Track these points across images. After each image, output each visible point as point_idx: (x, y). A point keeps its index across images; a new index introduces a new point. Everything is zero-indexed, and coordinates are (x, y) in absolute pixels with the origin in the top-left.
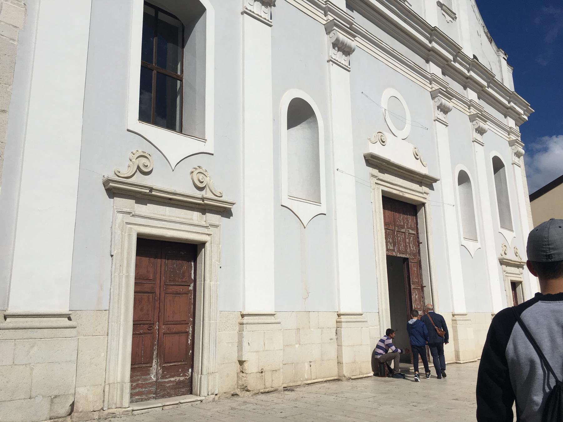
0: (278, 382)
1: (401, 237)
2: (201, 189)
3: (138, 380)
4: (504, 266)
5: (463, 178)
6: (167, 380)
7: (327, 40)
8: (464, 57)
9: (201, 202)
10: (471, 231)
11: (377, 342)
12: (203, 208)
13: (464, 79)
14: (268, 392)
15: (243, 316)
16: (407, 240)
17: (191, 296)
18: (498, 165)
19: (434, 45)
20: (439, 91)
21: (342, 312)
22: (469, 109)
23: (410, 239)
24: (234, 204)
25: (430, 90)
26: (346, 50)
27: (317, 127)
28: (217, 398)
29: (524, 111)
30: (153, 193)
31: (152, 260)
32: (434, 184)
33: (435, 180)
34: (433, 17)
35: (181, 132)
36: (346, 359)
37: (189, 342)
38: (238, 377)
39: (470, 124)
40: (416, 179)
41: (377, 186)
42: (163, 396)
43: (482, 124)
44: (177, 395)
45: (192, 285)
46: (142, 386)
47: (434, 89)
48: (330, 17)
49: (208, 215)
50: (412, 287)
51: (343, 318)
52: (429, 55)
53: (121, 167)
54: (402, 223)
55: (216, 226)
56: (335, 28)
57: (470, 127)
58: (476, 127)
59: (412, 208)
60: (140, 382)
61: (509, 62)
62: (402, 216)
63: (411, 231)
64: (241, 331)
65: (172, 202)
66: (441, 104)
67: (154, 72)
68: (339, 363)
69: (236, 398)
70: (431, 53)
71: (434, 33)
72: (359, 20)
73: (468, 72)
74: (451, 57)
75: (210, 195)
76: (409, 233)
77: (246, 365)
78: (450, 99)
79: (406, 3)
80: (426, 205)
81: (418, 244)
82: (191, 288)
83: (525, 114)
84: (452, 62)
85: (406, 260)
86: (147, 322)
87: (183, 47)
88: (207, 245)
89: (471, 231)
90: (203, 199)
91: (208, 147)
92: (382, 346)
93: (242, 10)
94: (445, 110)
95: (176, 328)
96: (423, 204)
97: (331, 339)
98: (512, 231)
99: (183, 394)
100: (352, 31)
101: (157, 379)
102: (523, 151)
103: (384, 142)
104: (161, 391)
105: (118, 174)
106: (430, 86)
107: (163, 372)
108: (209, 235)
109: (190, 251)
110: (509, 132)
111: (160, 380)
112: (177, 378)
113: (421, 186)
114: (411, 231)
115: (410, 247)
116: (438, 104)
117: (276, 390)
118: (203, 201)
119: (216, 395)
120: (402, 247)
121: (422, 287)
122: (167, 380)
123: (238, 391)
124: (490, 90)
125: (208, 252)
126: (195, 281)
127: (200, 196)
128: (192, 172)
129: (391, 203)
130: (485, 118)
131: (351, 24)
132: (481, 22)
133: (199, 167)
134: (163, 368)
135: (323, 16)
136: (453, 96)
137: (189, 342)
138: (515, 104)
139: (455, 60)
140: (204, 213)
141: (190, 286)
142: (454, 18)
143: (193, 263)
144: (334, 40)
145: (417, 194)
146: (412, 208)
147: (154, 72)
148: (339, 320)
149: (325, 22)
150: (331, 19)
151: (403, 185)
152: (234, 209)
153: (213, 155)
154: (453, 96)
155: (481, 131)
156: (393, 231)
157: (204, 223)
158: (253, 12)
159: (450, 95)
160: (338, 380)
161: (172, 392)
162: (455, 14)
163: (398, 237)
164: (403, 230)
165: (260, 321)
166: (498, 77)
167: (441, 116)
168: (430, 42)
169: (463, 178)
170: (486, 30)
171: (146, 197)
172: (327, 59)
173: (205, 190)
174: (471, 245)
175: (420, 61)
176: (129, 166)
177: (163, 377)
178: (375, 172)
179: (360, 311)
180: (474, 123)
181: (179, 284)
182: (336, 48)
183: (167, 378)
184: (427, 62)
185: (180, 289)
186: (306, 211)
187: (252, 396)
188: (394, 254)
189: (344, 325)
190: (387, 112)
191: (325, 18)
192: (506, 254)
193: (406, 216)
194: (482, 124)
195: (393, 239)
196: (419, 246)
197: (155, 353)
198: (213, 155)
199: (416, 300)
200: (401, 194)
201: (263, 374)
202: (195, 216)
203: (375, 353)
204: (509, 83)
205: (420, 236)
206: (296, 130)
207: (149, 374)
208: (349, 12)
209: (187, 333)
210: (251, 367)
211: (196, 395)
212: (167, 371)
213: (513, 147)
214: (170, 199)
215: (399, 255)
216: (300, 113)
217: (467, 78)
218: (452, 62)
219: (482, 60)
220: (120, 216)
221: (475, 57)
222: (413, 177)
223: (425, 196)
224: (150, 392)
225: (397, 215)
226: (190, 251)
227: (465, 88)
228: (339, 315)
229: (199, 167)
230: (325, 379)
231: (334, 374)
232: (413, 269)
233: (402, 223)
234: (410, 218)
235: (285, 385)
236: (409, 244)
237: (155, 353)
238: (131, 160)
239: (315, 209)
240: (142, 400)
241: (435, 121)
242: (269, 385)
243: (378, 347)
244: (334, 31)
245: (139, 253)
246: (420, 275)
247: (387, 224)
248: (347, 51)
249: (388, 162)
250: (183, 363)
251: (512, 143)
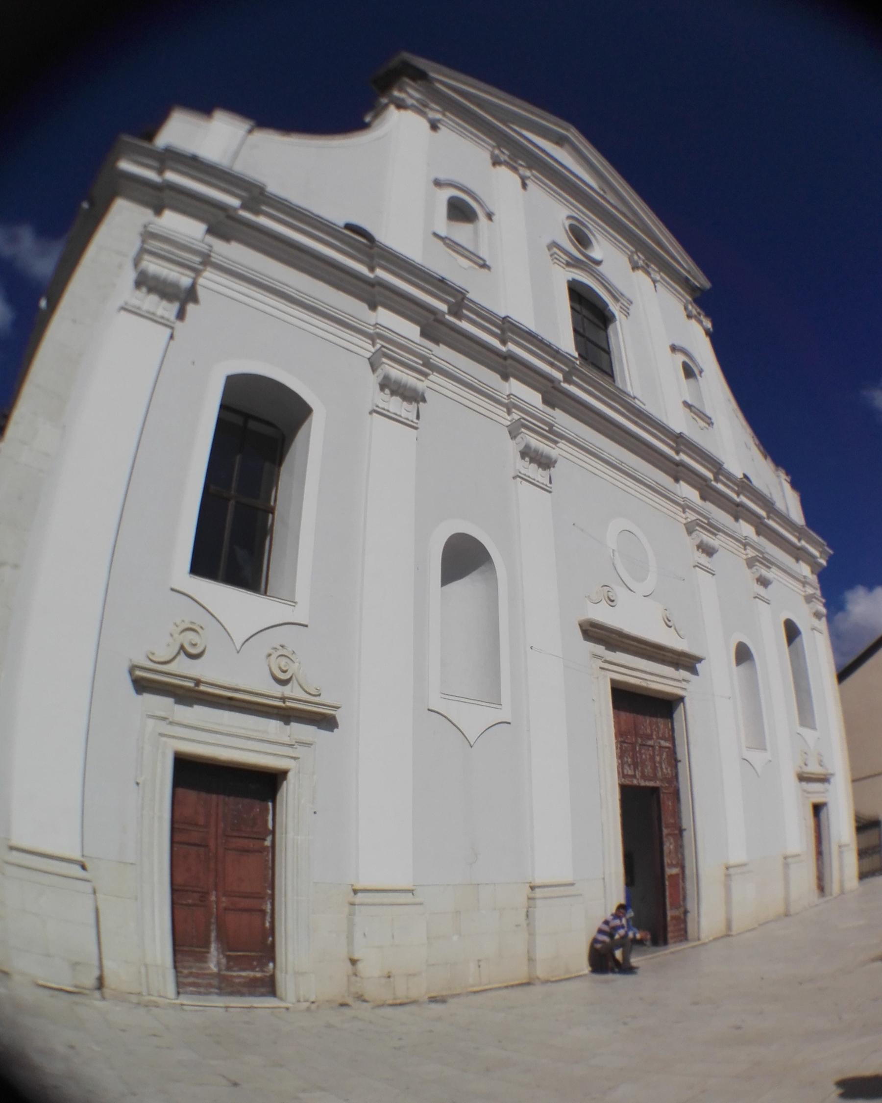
0: (419, 989)
1: (646, 754)
2: (284, 683)
3: (191, 967)
4: (804, 784)
5: (743, 654)
6: (235, 974)
7: (512, 448)
8: (729, 476)
9: (280, 704)
10: (758, 738)
11: (599, 924)
12: (286, 715)
13: (734, 506)
14: (401, 1004)
15: (355, 892)
16: (658, 758)
17: (267, 855)
18: (792, 632)
19: (683, 457)
20: (697, 523)
21: (538, 881)
22: (745, 549)
23: (661, 756)
24: (338, 708)
25: (684, 521)
26: (543, 460)
27: (496, 579)
28: (313, 1006)
29: (821, 553)
30: (202, 688)
31: (204, 795)
32: (698, 666)
33: (699, 660)
34: (679, 421)
35: (265, 593)
36: (542, 953)
37: (267, 925)
38: (349, 981)
39: (748, 572)
41: (603, 672)
42: (232, 994)
43: (764, 572)
44: (252, 994)
45: (269, 838)
46: (197, 976)
47: (689, 520)
48: (516, 415)
49: (294, 725)
50: (665, 831)
51: (538, 893)
52: (678, 471)
53: (155, 646)
54: (649, 731)
55: (308, 745)
56: (523, 430)
57: (749, 576)
58: (757, 575)
59: (665, 706)
60: (194, 970)
61: (794, 485)
62: (648, 720)
63: (663, 743)
64: (351, 914)
65: (233, 703)
66: (702, 542)
67: (232, 503)
68: (531, 960)
69: (345, 1010)
70: (680, 468)
71: (679, 441)
72: (562, 420)
73: (738, 495)
74: (710, 476)
75: (299, 694)
76: (660, 747)
77: (360, 966)
78: (715, 535)
79: (637, 401)
80: (687, 700)
81: (674, 761)
82: (268, 843)
83: (821, 557)
84: (713, 483)
85: (655, 790)
86: (199, 889)
87: (280, 464)
88: (290, 776)
89: (758, 738)
90: (283, 699)
91: (299, 614)
92: (608, 930)
93: (370, 409)
94: (709, 551)
95: (245, 903)
96: (681, 699)
97: (517, 926)
98: (814, 728)
99: (263, 995)
100: (552, 434)
101: (220, 970)
102: (823, 610)
103: (612, 601)
104: (225, 986)
105: (151, 657)
106: (684, 515)
107: (228, 962)
108: (295, 758)
109: (265, 784)
110: (804, 583)
111: (224, 973)
112: (251, 974)
113: (677, 669)
114: (663, 743)
115: (661, 768)
116: (698, 542)
117: (414, 1002)
118: (284, 702)
119: (313, 1002)
120: (648, 770)
121: (681, 831)
122: (235, 974)
123: (349, 1001)
124: (771, 523)
125: (291, 787)
126: (273, 833)
127: (279, 695)
128: (270, 655)
129: (626, 698)
130: (768, 562)
131: (551, 426)
132: (749, 431)
133: (282, 646)
134: (229, 958)
135: (506, 415)
136: (719, 530)
137: (267, 925)
138: (807, 542)
139: (717, 480)
140: (287, 723)
141: (264, 840)
142: (711, 424)
143: (270, 804)
144: (522, 447)
145: (672, 683)
146: (665, 706)
147: (232, 503)
148: (531, 895)
149: (509, 423)
150: (516, 417)
151: (648, 670)
152: (339, 715)
153: (306, 626)
154: (719, 530)
155: (764, 582)
156: (633, 745)
157: (286, 740)
158: (388, 411)
159: (713, 529)
160: (528, 984)
161: (245, 990)
162: (710, 418)
163: (641, 754)
164: (650, 743)
165: (385, 901)
166: (780, 505)
167: (703, 559)
168: (677, 453)
169: (743, 654)
170: (757, 442)
171: (190, 695)
172: (513, 474)
173: (289, 686)
174: (758, 758)
175: (666, 480)
176: (168, 645)
177: (229, 968)
178: (600, 649)
179: (569, 879)
180: (754, 569)
181: (247, 835)
182: (527, 459)
183: (234, 971)
184: (677, 480)
185: (251, 844)
186: (474, 718)
187: (373, 1008)
188: (635, 782)
189: (539, 903)
190: (617, 554)
191: (509, 418)
192: (806, 765)
193: (654, 719)
194: (764, 572)
195: (633, 758)
196: (676, 766)
197: (213, 935)
198: (306, 626)
199: (670, 852)
200: (644, 684)
201: (392, 979)
202: (272, 727)
203: (595, 941)
204: (797, 515)
205: (679, 750)
206: (458, 586)
207: (206, 962)
208: (548, 410)
209: (263, 912)
210: (370, 968)
211: (281, 999)
212: (233, 962)
213: (812, 604)
214: (230, 699)
215: (643, 783)
216: (463, 558)
217: (739, 505)
218: (713, 483)
219: (756, 483)
220: (151, 722)
221: (745, 476)
222: (664, 655)
223: (684, 685)
224: (210, 986)
225: (640, 718)
226: (265, 784)
227: (736, 519)
228: (532, 888)
229: (282, 646)
230: (505, 984)
231: (522, 974)
232: (667, 803)
233: (649, 731)
234: (661, 722)
235: (433, 994)
236: (660, 763)
237: (213, 935)
238: (172, 635)
239: (492, 715)
240: (200, 993)
242: (402, 994)
243: (600, 931)
244: (522, 435)
245: (177, 782)
246: (677, 813)
247: (620, 734)
248: (545, 463)
250: (260, 954)
251: (809, 599)
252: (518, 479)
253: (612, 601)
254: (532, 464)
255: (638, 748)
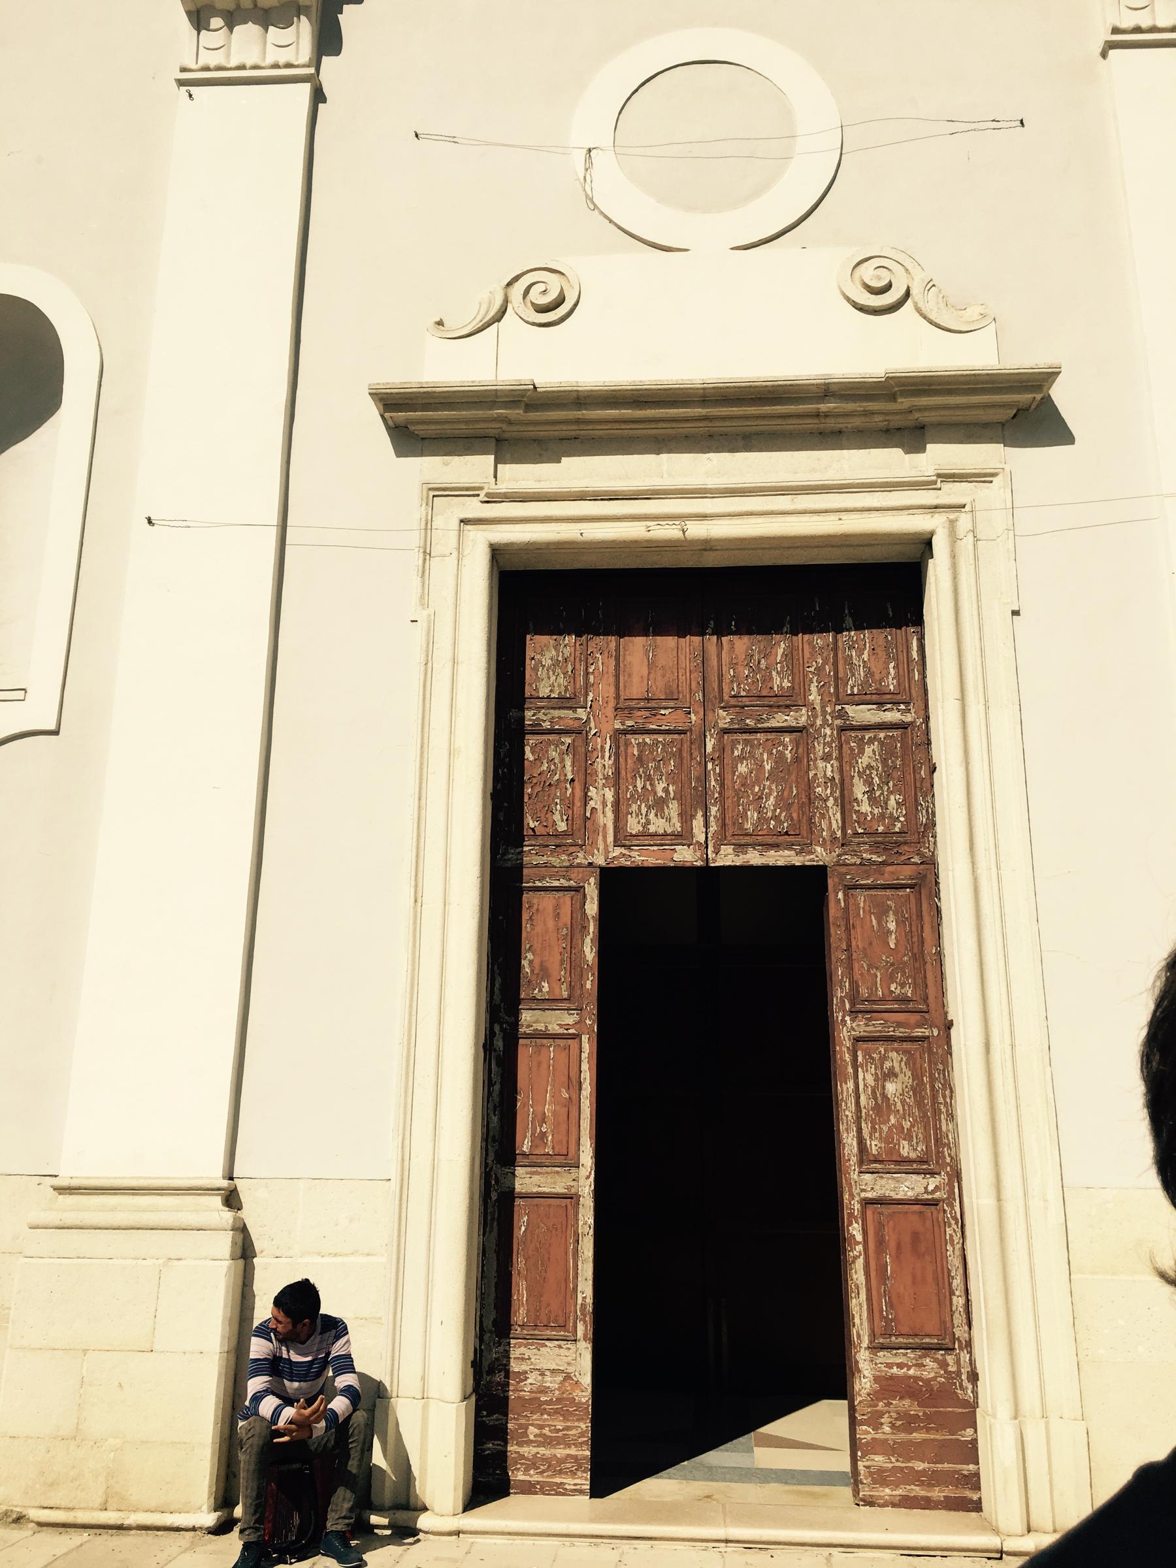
23: (845, 761)
33: (1050, 376)
40: (857, 422)
50: (847, 1029)
113: (916, 446)
115: (846, 803)
151: (712, 482)
178: (475, 468)
222: (817, 415)
241: (1104, 55)
249: (529, 399)
252: (183, 89)
253: (560, 301)
254: (236, 29)
255: (710, 744)
